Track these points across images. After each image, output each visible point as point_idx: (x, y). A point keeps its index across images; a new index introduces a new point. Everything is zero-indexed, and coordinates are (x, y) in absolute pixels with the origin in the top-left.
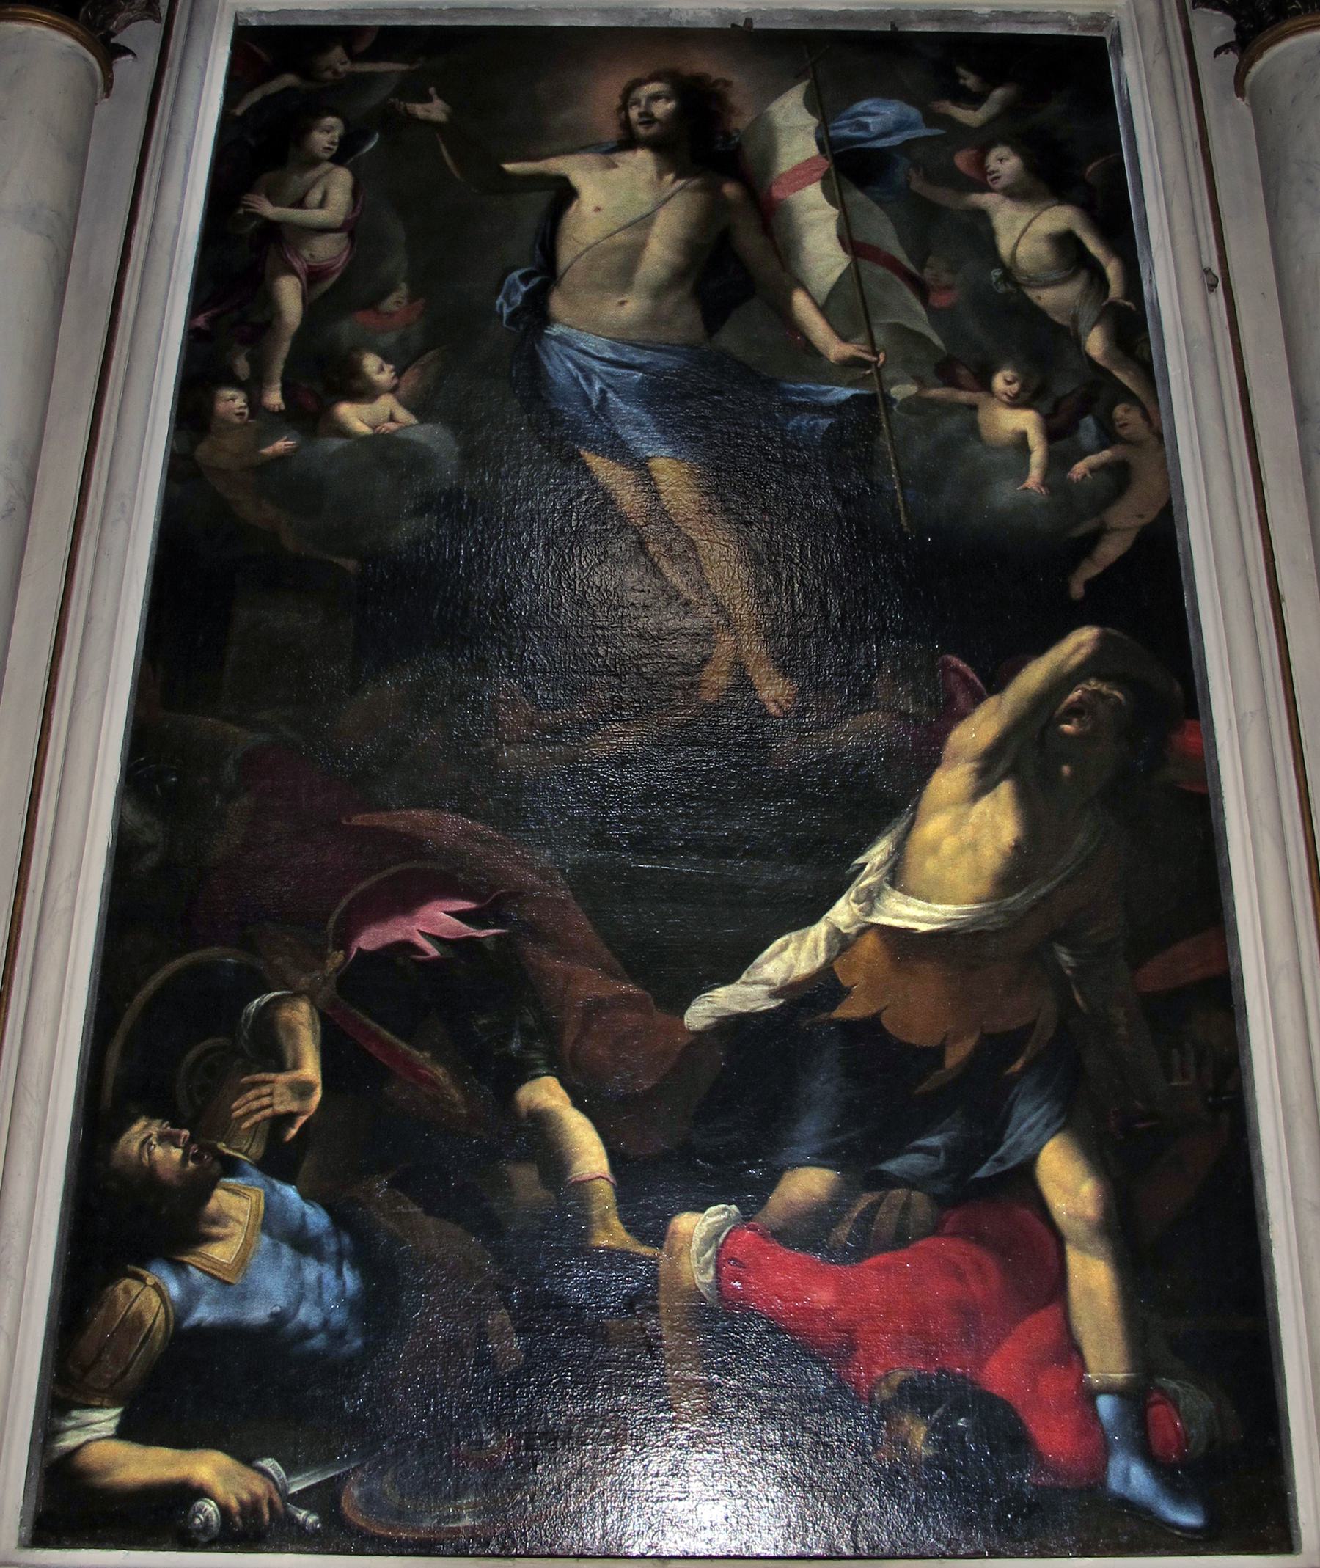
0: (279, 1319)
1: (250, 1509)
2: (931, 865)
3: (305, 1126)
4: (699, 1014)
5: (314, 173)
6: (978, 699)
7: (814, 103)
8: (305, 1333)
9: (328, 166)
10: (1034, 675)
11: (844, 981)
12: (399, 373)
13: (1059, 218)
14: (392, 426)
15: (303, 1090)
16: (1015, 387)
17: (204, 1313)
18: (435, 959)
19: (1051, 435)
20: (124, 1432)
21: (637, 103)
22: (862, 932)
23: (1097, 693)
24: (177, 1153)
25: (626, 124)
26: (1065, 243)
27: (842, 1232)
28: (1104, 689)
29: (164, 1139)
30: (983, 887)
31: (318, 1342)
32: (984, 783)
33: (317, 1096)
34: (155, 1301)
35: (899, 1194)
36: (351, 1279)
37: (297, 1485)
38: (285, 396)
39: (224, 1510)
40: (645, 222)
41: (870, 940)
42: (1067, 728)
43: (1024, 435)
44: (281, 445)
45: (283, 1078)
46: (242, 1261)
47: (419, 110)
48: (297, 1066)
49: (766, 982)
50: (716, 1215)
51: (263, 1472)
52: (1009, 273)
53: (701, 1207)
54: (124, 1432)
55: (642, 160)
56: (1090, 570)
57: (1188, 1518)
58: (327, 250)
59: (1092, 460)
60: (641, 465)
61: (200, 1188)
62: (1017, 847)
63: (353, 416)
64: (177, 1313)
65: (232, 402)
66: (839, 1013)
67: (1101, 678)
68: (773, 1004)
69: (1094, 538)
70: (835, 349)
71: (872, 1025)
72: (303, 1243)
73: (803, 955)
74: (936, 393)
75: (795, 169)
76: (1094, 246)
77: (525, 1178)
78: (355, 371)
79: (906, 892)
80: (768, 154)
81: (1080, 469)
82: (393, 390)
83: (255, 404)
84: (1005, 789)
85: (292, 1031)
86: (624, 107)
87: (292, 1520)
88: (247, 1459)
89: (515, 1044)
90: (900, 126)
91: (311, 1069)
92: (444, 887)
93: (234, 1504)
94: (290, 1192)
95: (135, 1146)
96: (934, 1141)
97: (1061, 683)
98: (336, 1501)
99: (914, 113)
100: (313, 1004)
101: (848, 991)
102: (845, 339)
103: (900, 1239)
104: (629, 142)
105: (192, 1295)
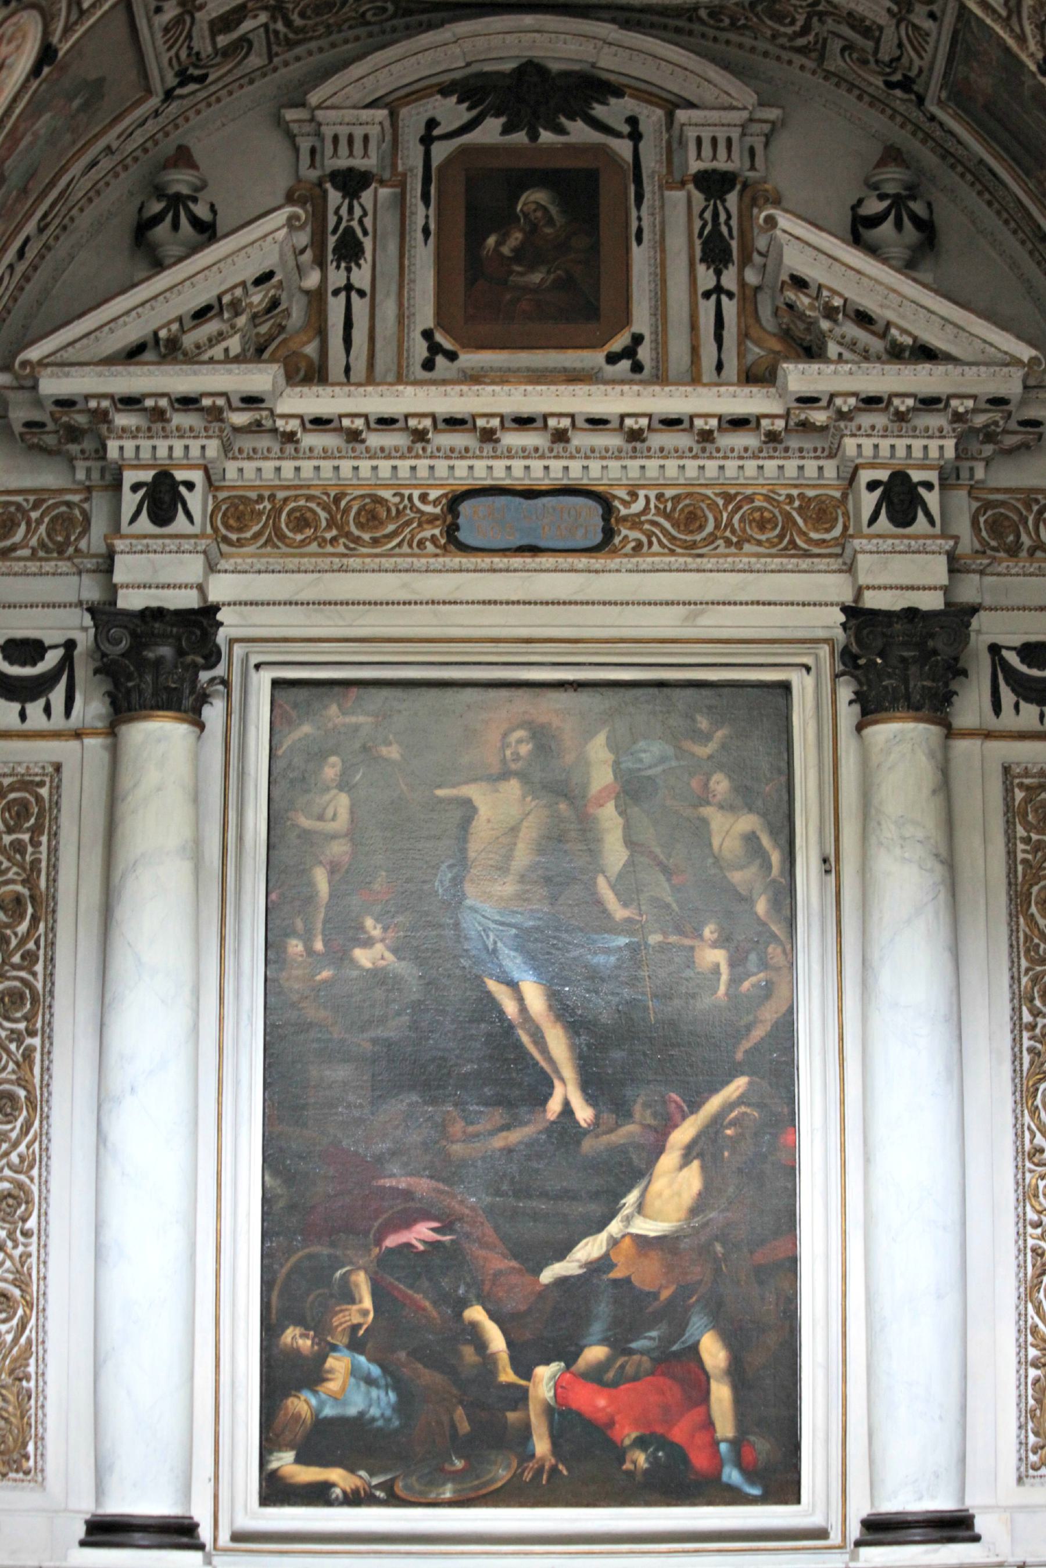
0: (362, 1414)
1: (356, 1492)
2: (657, 1203)
3: (367, 1330)
4: (547, 1276)
5: (327, 797)
6: (684, 1118)
7: (613, 745)
8: (373, 1419)
9: (334, 792)
10: (714, 1104)
11: (615, 1261)
12: (385, 929)
13: (748, 822)
14: (383, 963)
15: (365, 1313)
16: (716, 935)
17: (328, 1411)
18: (423, 1252)
19: (732, 964)
20: (299, 1460)
21: (509, 745)
22: (623, 1236)
23: (744, 1114)
24: (309, 1342)
25: (504, 761)
26: (751, 839)
27: (610, 1375)
28: (748, 1110)
29: (303, 1336)
30: (682, 1214)
31: (380, 1423)
32: (687, 1158)
33: (371, 1315)
34: (306, 1407)
35: (636, 1357)
36: (392, 1396)
37: (375, 1481)
38: (325, 945)
39: (344, 1492)
40: (514, 830)
41: (627, 1240)
42: (729, 1132)
43: (717, 966)
44: (326, 974)
45: (355, 1308)
46: (343, 1389)
47: (384, 751)
48: (361, 1302)
49: (578, 1261)
50: (556, 1367)
51: (361, 1477)
52: (717, 859)
53: (547, 1363)
54: (299, 1460)
55: (513, 787)
56: (746, 1045)
57: (755, 1491)
58: (339, 849)
59: (753, 979)
60: (513, 986)
61: (322, 1358)
62: (700, 1194)
63: (363, 957)
64: (316, 1414)
65: (295, 947)
66: (613, 1275)
67: (748, 1105)
68: (581, 1271)
69: (749, 1028)
70: (620, 913)
71: (628, 1281)
72: (370, 1381)
73: (596, 1247)
74: (673, 939)
75: (600, 792)
76: (766, 841)
77: (469, 1353)
78: (361, 928)
79: (645, 1216)
80: (585, 786)
81: (746, 985)
82: (382, 940)
83: (309, 951)
84: (696, 1164)
85: (357, 1285)
86: (504, 746)
87: (374, 1496)
88: (352, 1470)
89: (461, 1292)
90: (663, 759)
91: (367, 1303)
92: (425, 1215)
93: (348, 1490)
94: (362, 1359)
95: (289, 1340)
96: (654, 1334)
97: (730, 1106)
98: (392, 1487)
99: (670, 751)
100: (366, 1272)
101: (616, 1265)
102: (625, 905)
103: (635, 1378)
104: (505, 775)
105: (322, 1404)
